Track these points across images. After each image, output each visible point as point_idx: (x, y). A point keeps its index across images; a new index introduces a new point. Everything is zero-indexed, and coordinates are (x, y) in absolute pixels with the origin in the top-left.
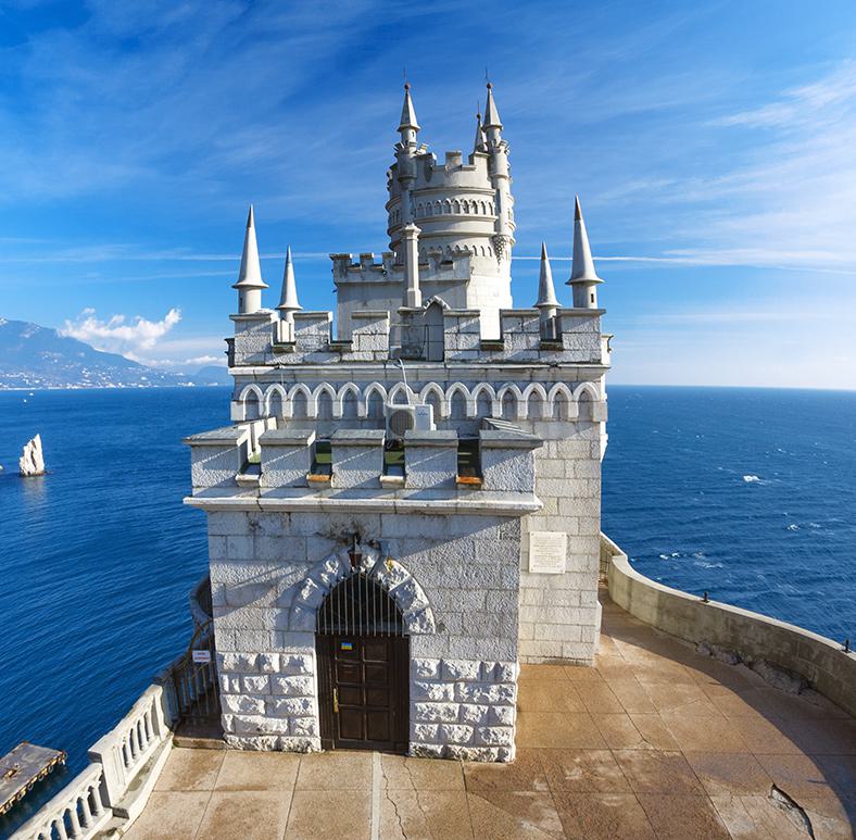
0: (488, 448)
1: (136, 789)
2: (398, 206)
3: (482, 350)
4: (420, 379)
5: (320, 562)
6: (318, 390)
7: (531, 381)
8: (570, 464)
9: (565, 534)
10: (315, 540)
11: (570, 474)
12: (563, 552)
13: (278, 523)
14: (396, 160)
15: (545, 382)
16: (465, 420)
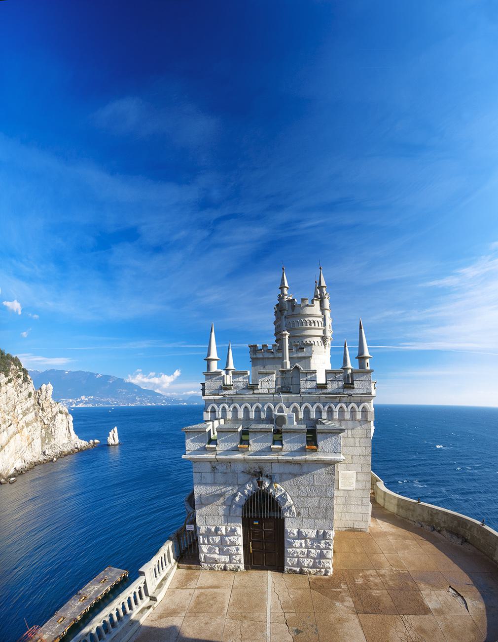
0: (320, 433)
1: (160, 588)
2: (279, 323)
3: (318, 388)
4: (289, 401)
5: (244, 484)
6: (243, 407)
7: (340, 402)
8: (357, 440)
9: (355, 472)
10: (242, 475)
11: (357, 444)
12: (354, 480)
13: (225, 467)
14: (278, 302)
15: (346, 403)
16: (309, 420)
